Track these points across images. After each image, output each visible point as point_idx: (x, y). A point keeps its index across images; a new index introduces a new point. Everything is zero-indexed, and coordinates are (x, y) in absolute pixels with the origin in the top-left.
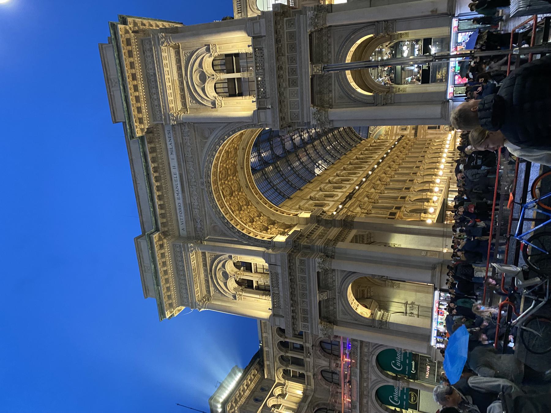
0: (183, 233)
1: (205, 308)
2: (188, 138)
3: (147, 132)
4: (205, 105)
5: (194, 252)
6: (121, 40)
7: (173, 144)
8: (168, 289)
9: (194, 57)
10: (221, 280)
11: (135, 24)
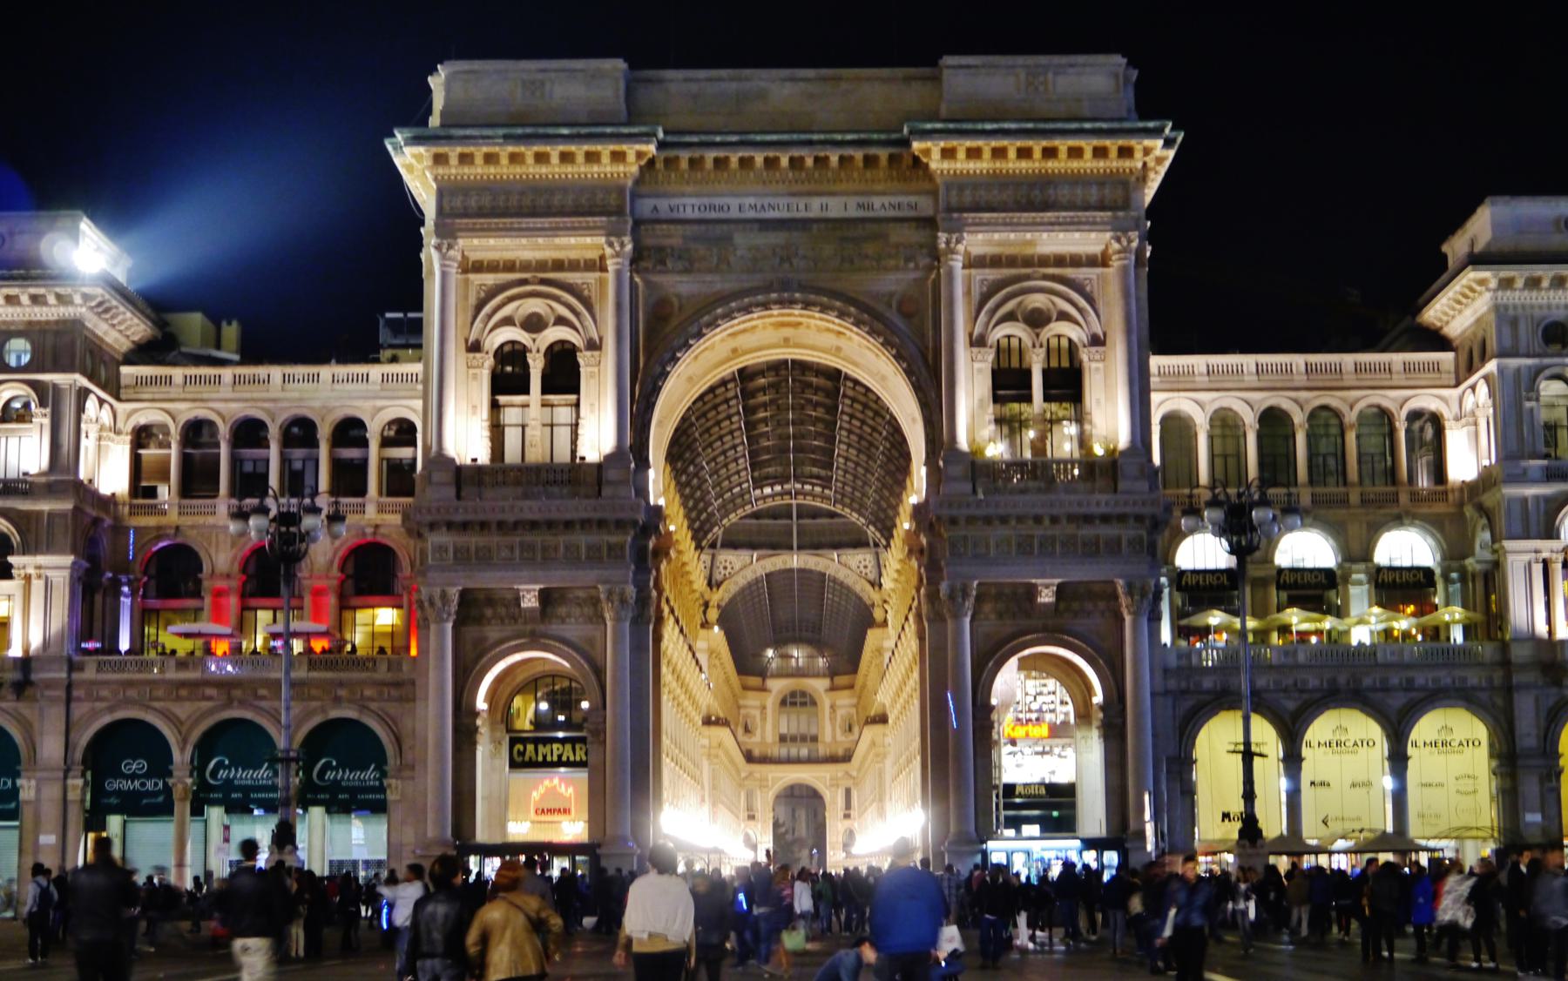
1: (443, 266)
2: (902, 263)
3: (916, 160)
7: (882, 214)
8: (490, 159)
9: (1082, 303)
10: (518, 308)
11: (1159, 161)
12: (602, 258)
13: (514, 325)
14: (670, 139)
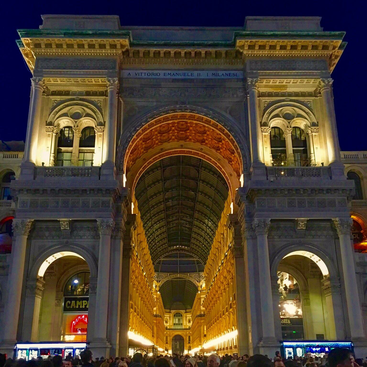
0: (125, 73)
1: (35, 87)
4: (263, 116)
5: (108, 83)
6: (329, 41)
7: (223, 77)
8: (59, 46)
9: (307, 110)
12: (106, 91)
13: (68, 116)
14: (135, 42)
